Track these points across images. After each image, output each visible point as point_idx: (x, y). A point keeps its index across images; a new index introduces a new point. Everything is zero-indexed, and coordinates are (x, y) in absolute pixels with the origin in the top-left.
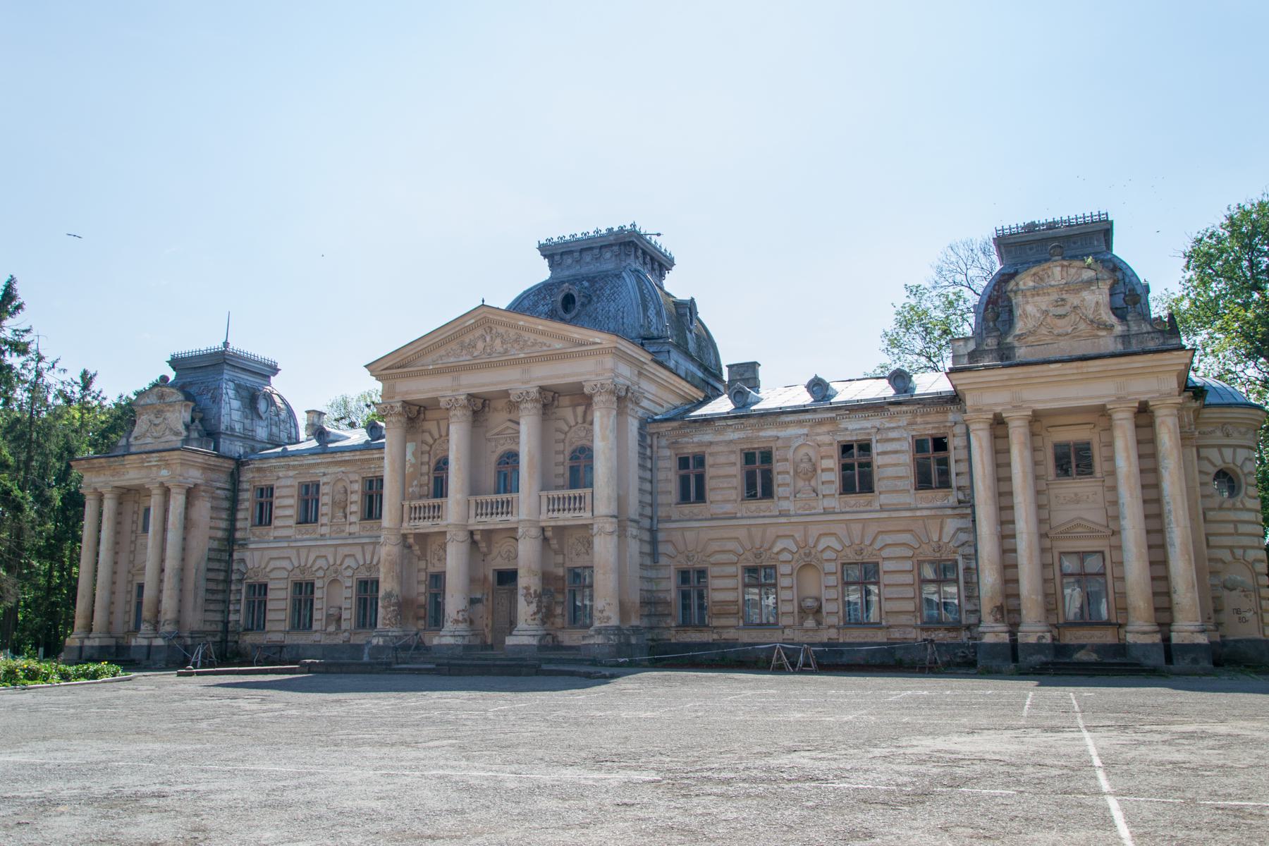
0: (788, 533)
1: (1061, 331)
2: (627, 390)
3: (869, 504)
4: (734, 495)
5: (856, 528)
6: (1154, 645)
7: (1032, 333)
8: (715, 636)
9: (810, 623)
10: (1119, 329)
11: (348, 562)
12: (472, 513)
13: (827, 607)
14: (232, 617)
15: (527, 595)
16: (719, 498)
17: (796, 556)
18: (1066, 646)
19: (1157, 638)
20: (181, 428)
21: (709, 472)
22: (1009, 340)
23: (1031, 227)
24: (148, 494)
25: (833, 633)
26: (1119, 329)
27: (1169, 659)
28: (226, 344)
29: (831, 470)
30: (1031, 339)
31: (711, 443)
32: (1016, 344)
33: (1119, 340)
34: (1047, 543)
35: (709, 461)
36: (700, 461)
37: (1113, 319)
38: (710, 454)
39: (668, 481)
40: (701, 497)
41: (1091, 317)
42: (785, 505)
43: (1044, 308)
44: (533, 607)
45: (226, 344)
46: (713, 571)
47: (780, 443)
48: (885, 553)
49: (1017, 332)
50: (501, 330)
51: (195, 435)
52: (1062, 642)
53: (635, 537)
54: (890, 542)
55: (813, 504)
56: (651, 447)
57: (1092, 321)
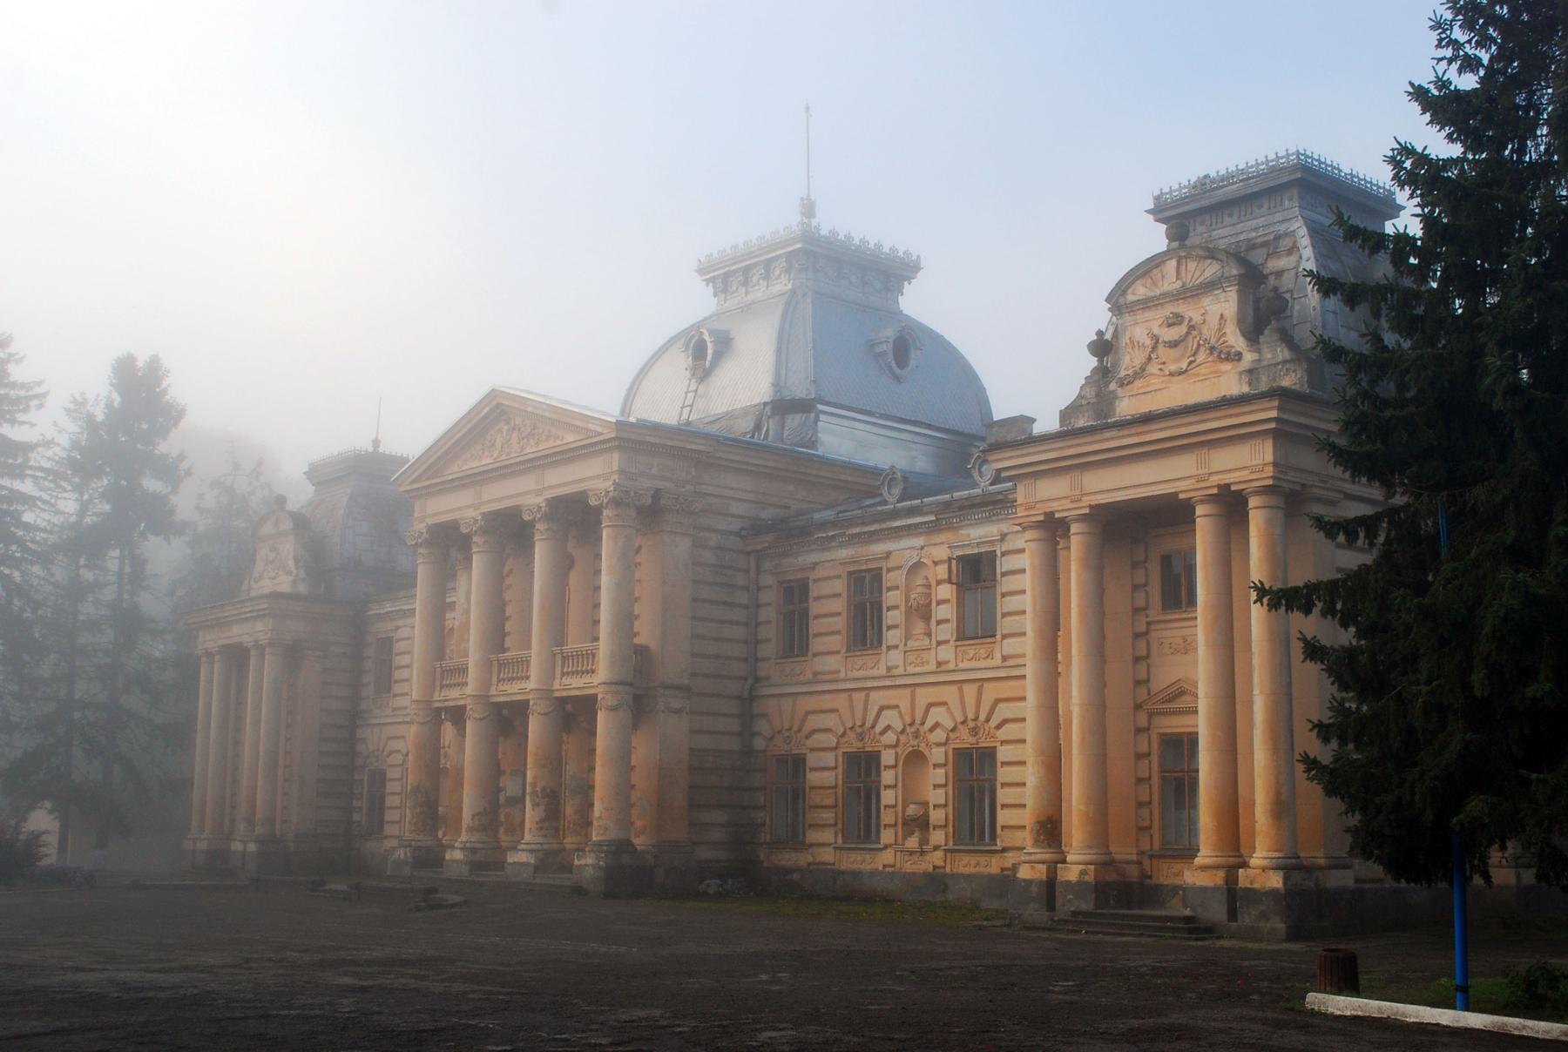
0: (830, 706)
1: (1173, 368)
2: (657, 495)
3: (990, 656)
4: (836, 642)
5: (970, 691)
6: (1216, 888)
7: (1140, 373)
8: (810, 859)
9: (912, 842)
10: (1249, 357)
11: (937, 714)
12: (495, 678)
13: (936, 816)
14: (356, 817)
15: (534, 793)
16: (822, 649)
17: (903, 738)
18: (1158, 886)
19: (1218, 878)
20: (291, 563)
21: (815, 608)
22: (1113, 386)
23: (1204, 185)
24: (247, 651)
25: (937, 858)
26: (1249, 357)
27: (1232, 914)
28: (376, 442)
29: (946, 601)
30: (1138, 383)
31: (815, 566)
32: (1120, 392)
33: (1245, 378)
34: (1143, 720)
35: (814, 590)
36: (804, 587)
37: (1236, 340)
38: (817, 581)
39: (768, 622)
40: (804, 650)
41: (1213, 341)
42: (895, 658)
43: (1156, 331)
44: (540, 812)
45: (376, 442)
46: (812, 759)
47: (891, 563)
48: (1002, 734)
49: (1122, 374)
50: (518, 421)
51: (302, 574)
52: (1155, 881)
53: (678, 711)
54: (1008, 715)
55: (925, 655)
56: (747, 571)
57: (1212, 349)
